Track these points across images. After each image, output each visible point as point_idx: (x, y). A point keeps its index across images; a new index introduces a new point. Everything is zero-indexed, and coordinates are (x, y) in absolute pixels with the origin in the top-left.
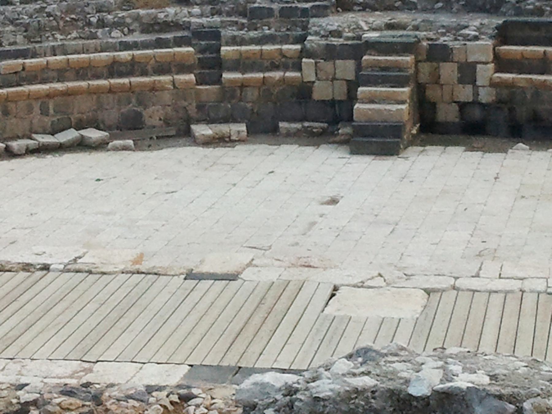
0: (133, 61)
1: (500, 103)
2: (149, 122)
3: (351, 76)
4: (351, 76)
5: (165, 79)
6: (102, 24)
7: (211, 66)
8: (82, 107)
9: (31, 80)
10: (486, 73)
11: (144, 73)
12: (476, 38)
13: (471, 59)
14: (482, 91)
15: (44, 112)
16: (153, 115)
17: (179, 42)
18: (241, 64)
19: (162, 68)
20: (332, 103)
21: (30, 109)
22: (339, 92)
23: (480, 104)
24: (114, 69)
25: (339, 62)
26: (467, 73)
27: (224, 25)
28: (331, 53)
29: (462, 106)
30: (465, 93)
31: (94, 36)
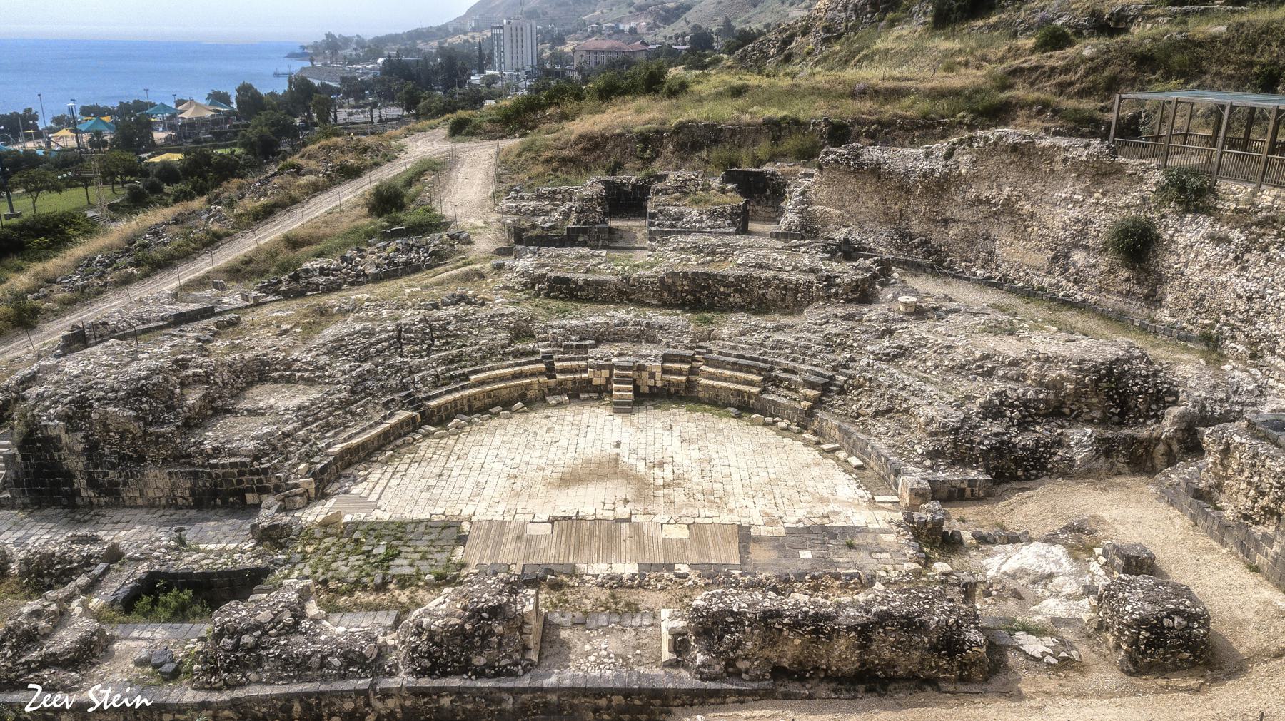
5: (535, 380)
10: (658, 376)
16: (531, 394)
18: (563, 371)
19: (533, 374)
22: (603, 382)
24: (515, 376)
26: (652, 376)
27: (554, 352)
30: (651, 382)
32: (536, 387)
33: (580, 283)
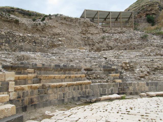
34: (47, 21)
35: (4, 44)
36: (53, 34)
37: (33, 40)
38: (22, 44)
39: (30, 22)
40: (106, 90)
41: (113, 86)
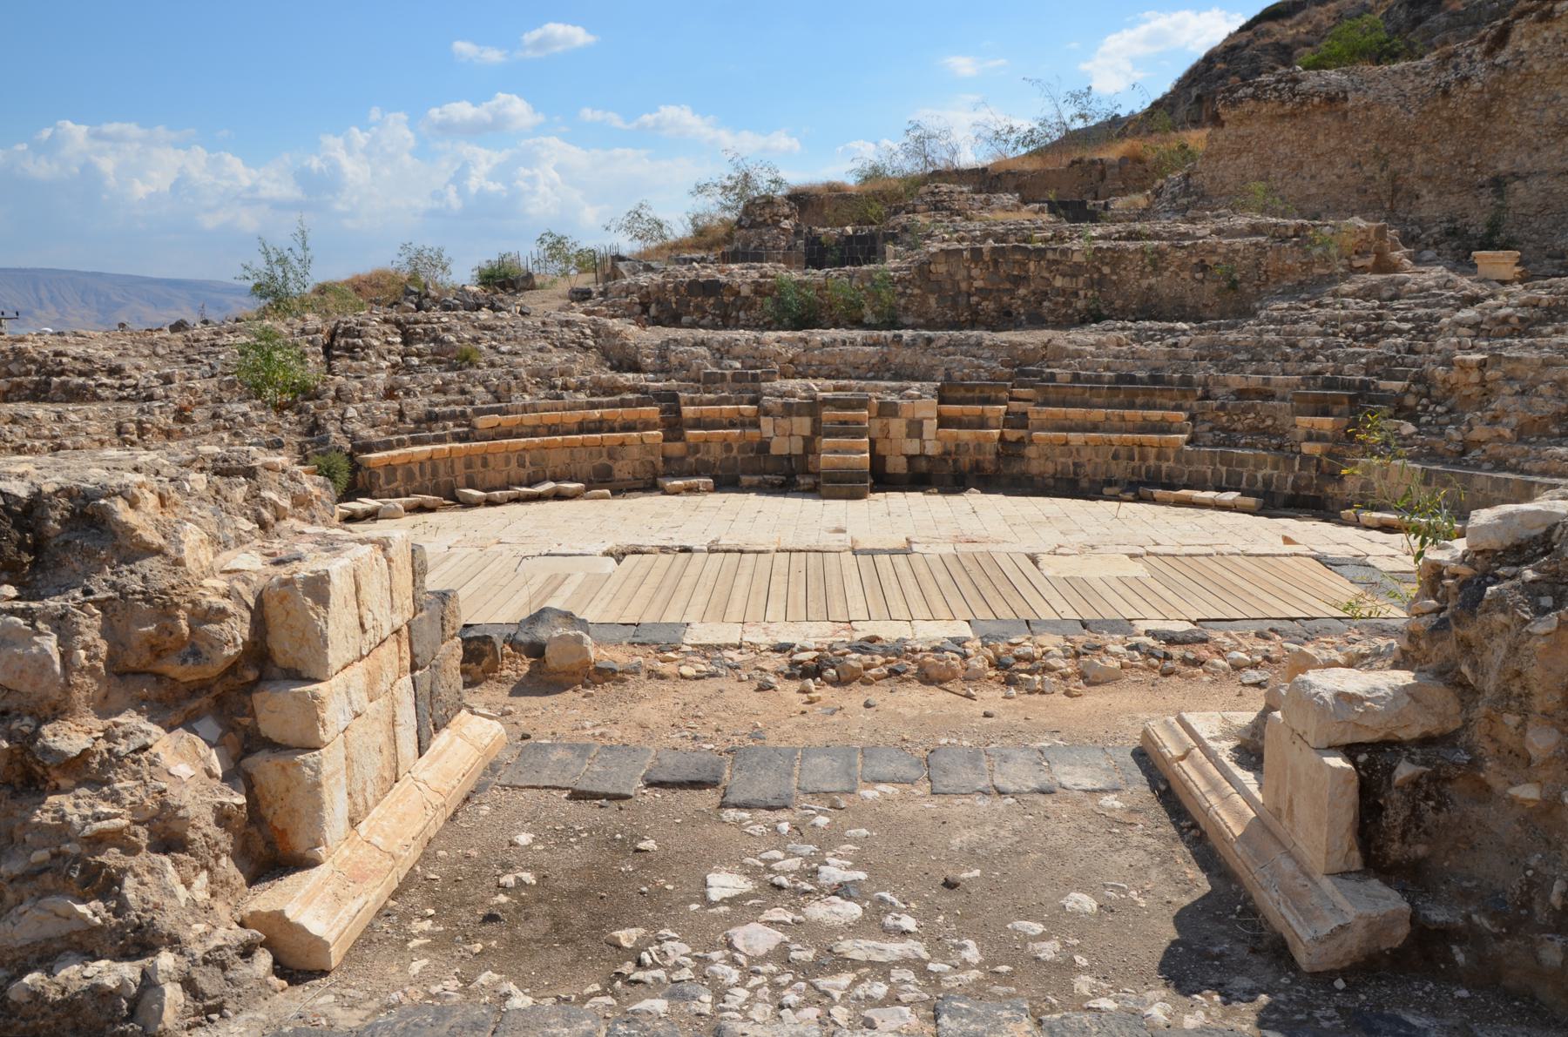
0: (601, 421)
1: (946, 453)
2: (617, 475)
3: (807, 432)
4: (807, 432)
6: (565, 387)
7: (674, 426)
8: (557, 460)
9: (509, 434)
10: (930, 427)
11: (612, 430)
12: (920, 397)
13: (919, 415)
14: (928, 444)
15: (521, 465)
16: (622, 469)
17: (640, 403)
20: (789, 457)
21: (507, 462)
22: (796, 447)
23: (928, 457)
24: (583, 428)
25: (795, 419)
26: (915, 428)
28: (789, 410)
29: (911, 458)
30: (913, 447)
31: (559, 397)
32: (635, 452)
33: (745, 291)
34: (1525, 45)
35: (1082, 293)
36: (1556, 124)
37: (1195, 260)
38: (1153, 280)
39: (1418, 80)
40: (1241, 474)
41: (1275, 467)
